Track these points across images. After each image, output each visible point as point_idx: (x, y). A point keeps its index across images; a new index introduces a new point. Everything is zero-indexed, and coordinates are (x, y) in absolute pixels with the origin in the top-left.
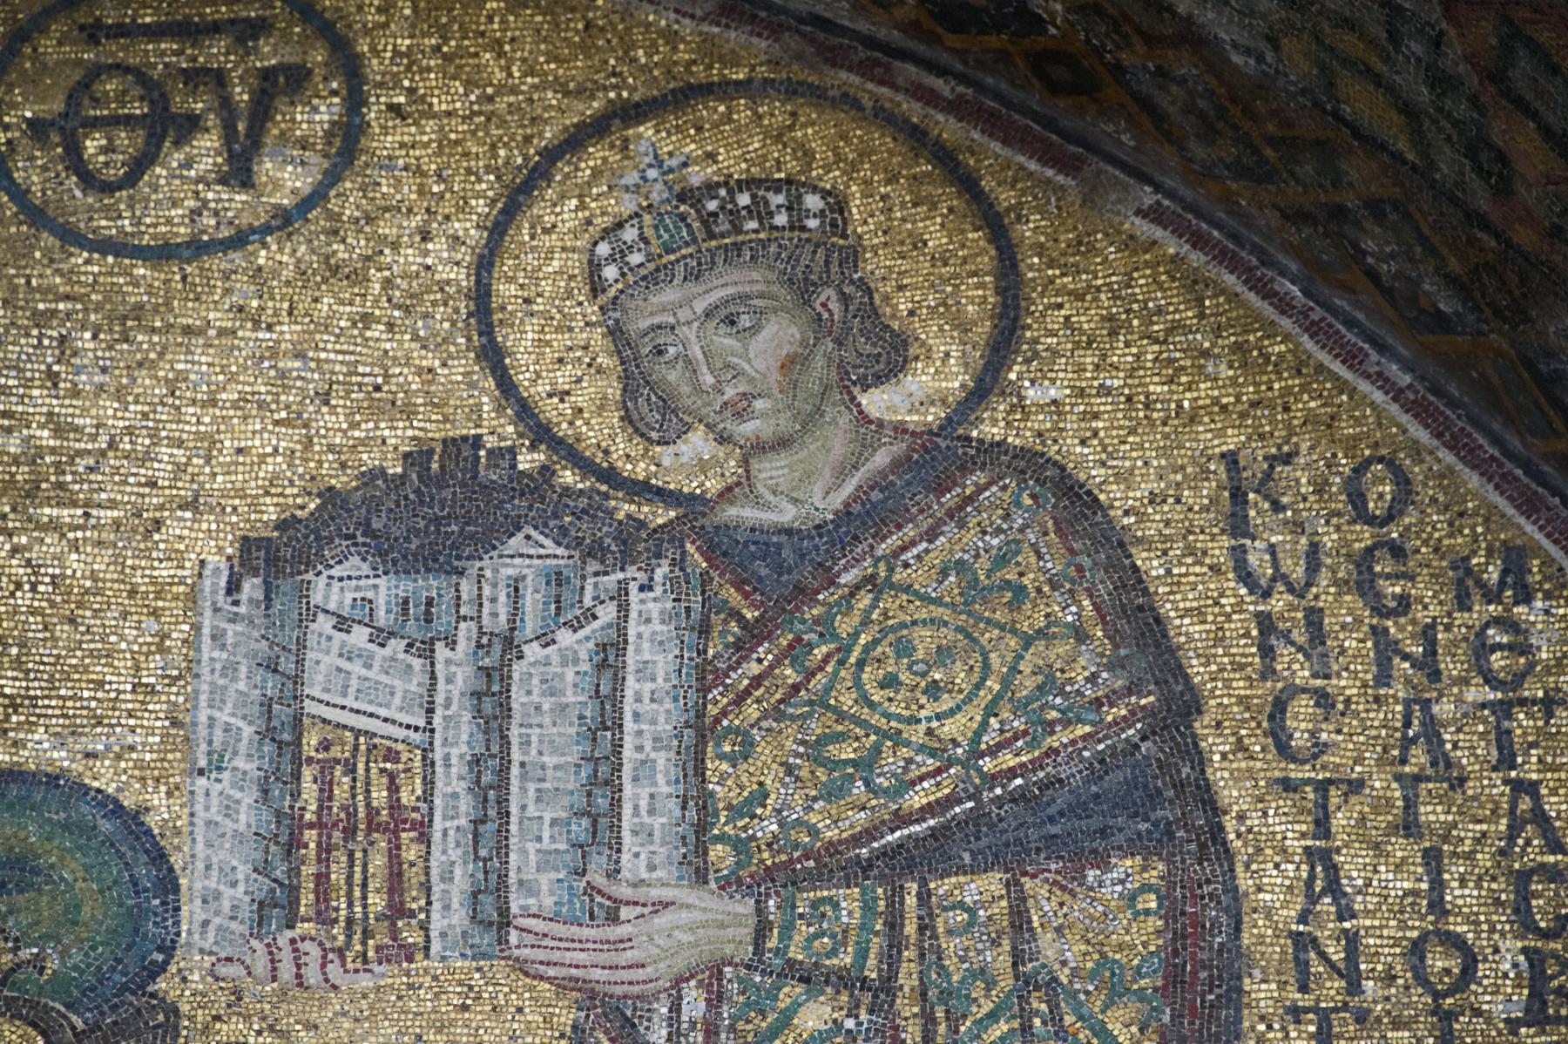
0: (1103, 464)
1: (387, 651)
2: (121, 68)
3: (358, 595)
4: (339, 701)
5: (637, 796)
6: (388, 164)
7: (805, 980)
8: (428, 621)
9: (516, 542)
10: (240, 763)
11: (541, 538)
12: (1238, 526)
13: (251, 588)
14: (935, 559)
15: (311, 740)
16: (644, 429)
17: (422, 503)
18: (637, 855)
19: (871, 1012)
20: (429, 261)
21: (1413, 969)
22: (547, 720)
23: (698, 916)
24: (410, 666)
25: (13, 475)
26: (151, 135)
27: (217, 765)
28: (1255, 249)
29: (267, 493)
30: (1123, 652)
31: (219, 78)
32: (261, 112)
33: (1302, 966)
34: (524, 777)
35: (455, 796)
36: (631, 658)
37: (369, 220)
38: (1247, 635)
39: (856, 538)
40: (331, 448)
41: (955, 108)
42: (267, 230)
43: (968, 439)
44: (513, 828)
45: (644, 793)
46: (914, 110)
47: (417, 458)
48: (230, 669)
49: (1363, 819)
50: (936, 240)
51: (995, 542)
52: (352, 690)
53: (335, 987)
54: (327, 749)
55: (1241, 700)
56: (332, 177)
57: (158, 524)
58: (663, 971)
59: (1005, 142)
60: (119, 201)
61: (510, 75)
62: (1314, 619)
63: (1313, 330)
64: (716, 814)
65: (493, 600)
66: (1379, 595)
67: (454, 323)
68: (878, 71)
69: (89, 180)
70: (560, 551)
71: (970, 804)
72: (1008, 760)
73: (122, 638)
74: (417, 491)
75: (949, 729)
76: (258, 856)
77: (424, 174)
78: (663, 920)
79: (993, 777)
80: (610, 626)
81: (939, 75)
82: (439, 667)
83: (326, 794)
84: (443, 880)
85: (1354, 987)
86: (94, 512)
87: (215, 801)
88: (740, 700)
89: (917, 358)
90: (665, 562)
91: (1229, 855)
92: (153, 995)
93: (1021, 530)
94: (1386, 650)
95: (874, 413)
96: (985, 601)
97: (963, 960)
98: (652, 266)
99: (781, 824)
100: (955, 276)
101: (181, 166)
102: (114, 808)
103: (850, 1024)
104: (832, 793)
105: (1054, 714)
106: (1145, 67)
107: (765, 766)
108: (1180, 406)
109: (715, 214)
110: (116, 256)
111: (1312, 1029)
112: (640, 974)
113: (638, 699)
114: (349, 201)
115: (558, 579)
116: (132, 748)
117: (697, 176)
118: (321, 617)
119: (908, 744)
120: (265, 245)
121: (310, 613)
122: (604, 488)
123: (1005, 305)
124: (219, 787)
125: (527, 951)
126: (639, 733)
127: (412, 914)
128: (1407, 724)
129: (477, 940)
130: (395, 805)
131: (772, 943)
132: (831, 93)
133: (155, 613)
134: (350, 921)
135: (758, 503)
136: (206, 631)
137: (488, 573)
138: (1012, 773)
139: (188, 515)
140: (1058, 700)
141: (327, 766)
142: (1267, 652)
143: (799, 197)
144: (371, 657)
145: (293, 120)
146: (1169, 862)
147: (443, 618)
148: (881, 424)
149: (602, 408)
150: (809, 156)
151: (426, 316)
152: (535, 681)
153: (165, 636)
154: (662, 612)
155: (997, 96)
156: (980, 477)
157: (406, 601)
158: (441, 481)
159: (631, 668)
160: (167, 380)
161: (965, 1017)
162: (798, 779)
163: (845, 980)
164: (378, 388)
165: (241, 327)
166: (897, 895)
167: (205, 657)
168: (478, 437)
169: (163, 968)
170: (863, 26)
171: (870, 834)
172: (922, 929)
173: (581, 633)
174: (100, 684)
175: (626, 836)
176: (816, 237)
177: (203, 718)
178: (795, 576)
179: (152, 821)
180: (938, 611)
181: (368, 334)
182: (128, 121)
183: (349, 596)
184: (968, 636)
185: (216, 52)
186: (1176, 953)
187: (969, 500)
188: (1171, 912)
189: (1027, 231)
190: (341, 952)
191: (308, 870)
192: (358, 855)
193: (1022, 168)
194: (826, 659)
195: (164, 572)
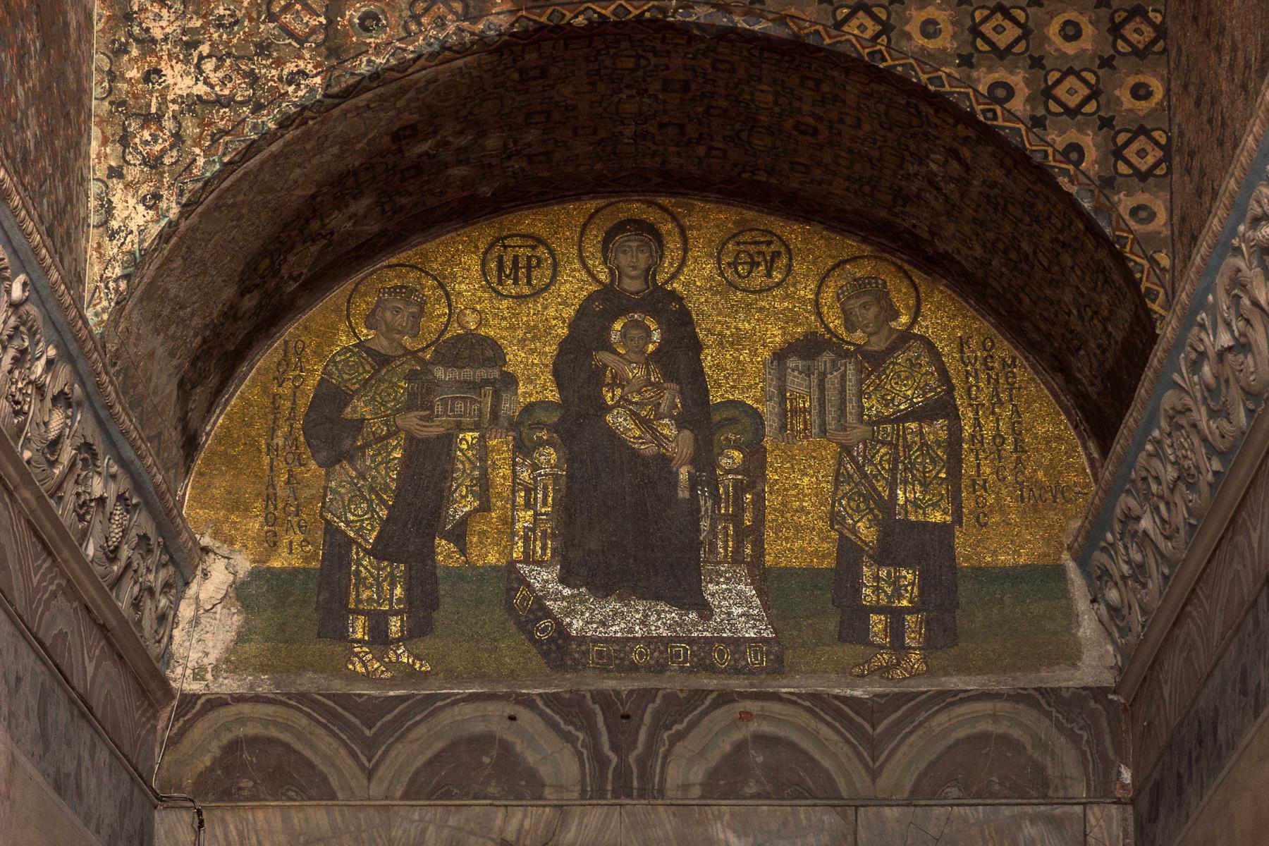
75: (909, 393)
85: (983, 445)
91: (960, 419)
102: (750, 406)
104: (887, 406)
171: (894, 413)
188: (949, 429)
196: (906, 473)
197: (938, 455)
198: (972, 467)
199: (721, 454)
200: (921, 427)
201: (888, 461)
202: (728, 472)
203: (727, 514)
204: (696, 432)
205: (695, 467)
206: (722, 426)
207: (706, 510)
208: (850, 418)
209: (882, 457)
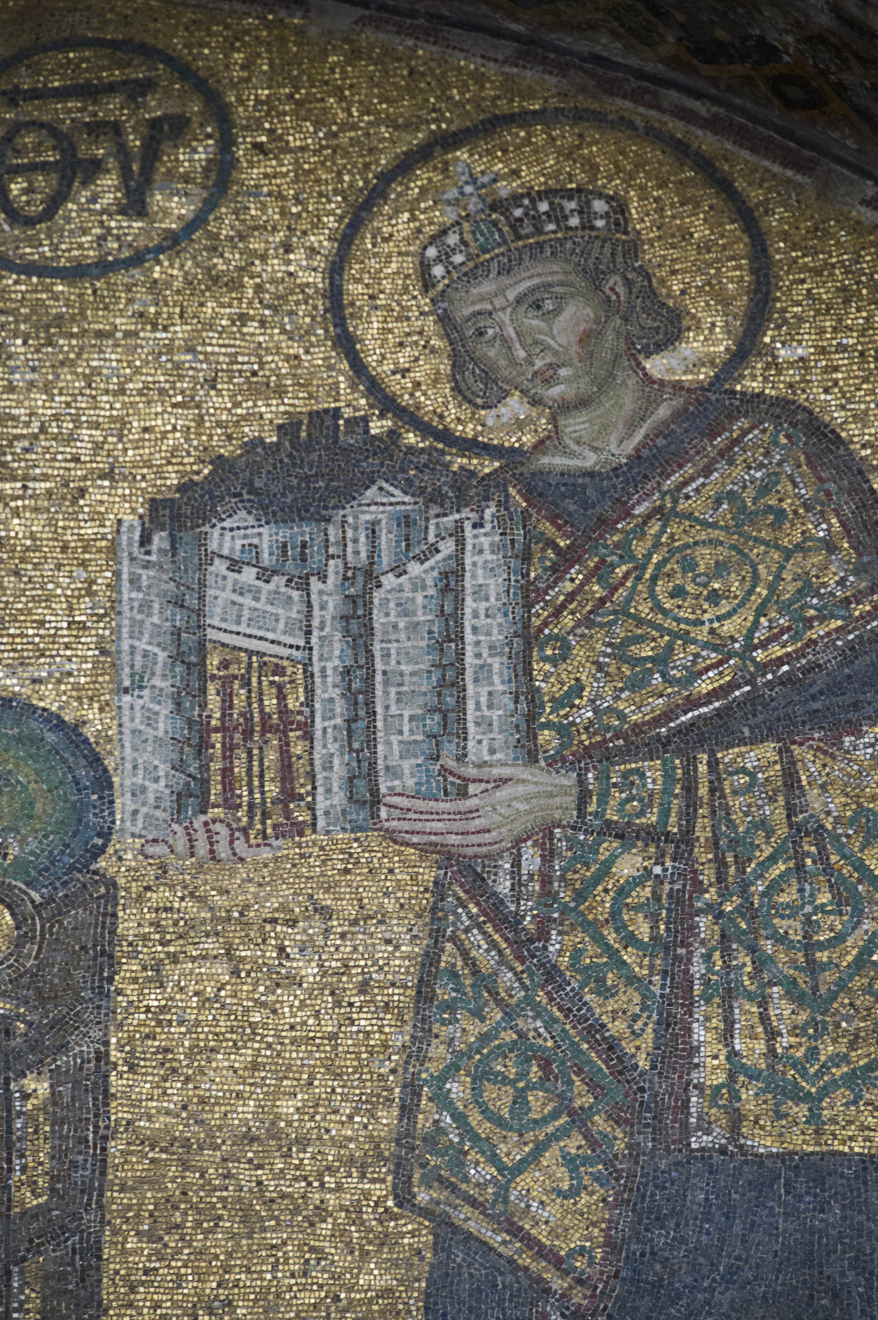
0: (843, 407)
1: (271, 586)
3: (246, 542)
4: (235, 628)
5: (478, 694)
6: (255, 192)
7: (620, 836)
8: (304, 560)
9: (371, 493)
10: (157, 682)
11: (391, 489)
13: (159, 540)
14: (710, 491)
15: (213, 661)
16: (471, 397)
18: (480, 742)
19: (674, 860)
20: (292, 269)
22: (403, 636)
23: (532, 788)
24: (290, 598)
26: (63, 177)
29: (169, 463)
30: (865, 559)
31: (116, 129)
34: (386, 683)
35: (331, 700)
36: (468, 583)
37: (242, 237)
39: (646, 477)
40: (219, 424)
41: (712, 125)
42: (160, 249)
43: (734, 392)
44: (380, 724)
45: (484, 691)
46: (677, 128)
48: (145, 607)
51: (759, 475)
52: (244, 619)
53: (242, 860)
54: (226, 667)
56: (210, 205)
57: (82, 492)
58: (505, 834)
59: (753, 150)
60: (39, 232)
61: (350, 115)
65: (355, 541)
67: (313, 318)
68: (648, 97)
70: (407, 499)
71: (747, 688)
72: (777, 651)
73: (58, 585)
74: (290, 456)
75: (727, 628)
76: (175, 756)
77: (284, 199)
78: (503, 793)
79: (765, 665)
80: (450, 557)
82: (314, 597)
83: (227, 704)
84: (324, 769)
86: (31, 484)
87: (138, 714)
88: (558, 612)
89: (689, 329)
90: (492, 504)
92: (95, 872)
93: (780, 464)
95: (656, 375)
96: (752, 523)
97: (746, 814)
98: (471, 264)
99: (595, 711)
100: (717, 260)
101: (88, 201)
102: (56, 722)
103: (658, 870)
104: (636, 684)
105: (812, 612)
106: (862, 84)
109: (520, 220)
110: (39, 276)
112: (487, 838)
115: (406, 521)
116: (70, 674)
117: (504, 189)
118: (217, 561)
119: (695, 642)
120: (159, 262)
121: (210, 558)
122: (440, 446)
123: (758, 283)
124: (141, 702)
125: (395, 823)
126: (478, 643)
129: (354, 816)
130: (283, 710)
131: (592, 808)
132: (610, 117)
133: (84, 564)
134: (251, 805)
135: (566, 452)
136: (125, 576)
137: (350, 520)
138: (780, 662)
139: (106, 483)
140: (815, 601)
143: (588, 203)
144: (259, 591)
145: (177, 160)
147: (316, 559)
148: (662, 383)
149: (436, 381)
150: (593, 169)
151: (291, 313)
152: (392, 605)
153: (93, 582)
154: (492, 544)
155: (745, 113)
156: (743, 423)
157: (285, 545)
158: (309, 447)
159: (468, 591)
160: (84, 375)
161: (750, 860)
162: (607, 674)
165: (143, 329)
166: (691, 764)
167: (125, 597)
168: (337, 410)
169: (102, 850)
170: (633, 61)
171: (667, 715)
172: (712, 791)
173: (427, 565)
174: (41, 623)
176: (602, 234)
177: (125, 647)
178: (598, 510)
179: (89, 732)
180: (716, 533)
181: (245, 330)
182: (44, 167)
183: (239, 543)
184: (740, 552)
187: (736, 442)
190: (245, 831)
192: (256, 751)
193: (767, 170)
194: (626, 576)
195: (89, 531)
196: (727, 953)
209: (622, 892)
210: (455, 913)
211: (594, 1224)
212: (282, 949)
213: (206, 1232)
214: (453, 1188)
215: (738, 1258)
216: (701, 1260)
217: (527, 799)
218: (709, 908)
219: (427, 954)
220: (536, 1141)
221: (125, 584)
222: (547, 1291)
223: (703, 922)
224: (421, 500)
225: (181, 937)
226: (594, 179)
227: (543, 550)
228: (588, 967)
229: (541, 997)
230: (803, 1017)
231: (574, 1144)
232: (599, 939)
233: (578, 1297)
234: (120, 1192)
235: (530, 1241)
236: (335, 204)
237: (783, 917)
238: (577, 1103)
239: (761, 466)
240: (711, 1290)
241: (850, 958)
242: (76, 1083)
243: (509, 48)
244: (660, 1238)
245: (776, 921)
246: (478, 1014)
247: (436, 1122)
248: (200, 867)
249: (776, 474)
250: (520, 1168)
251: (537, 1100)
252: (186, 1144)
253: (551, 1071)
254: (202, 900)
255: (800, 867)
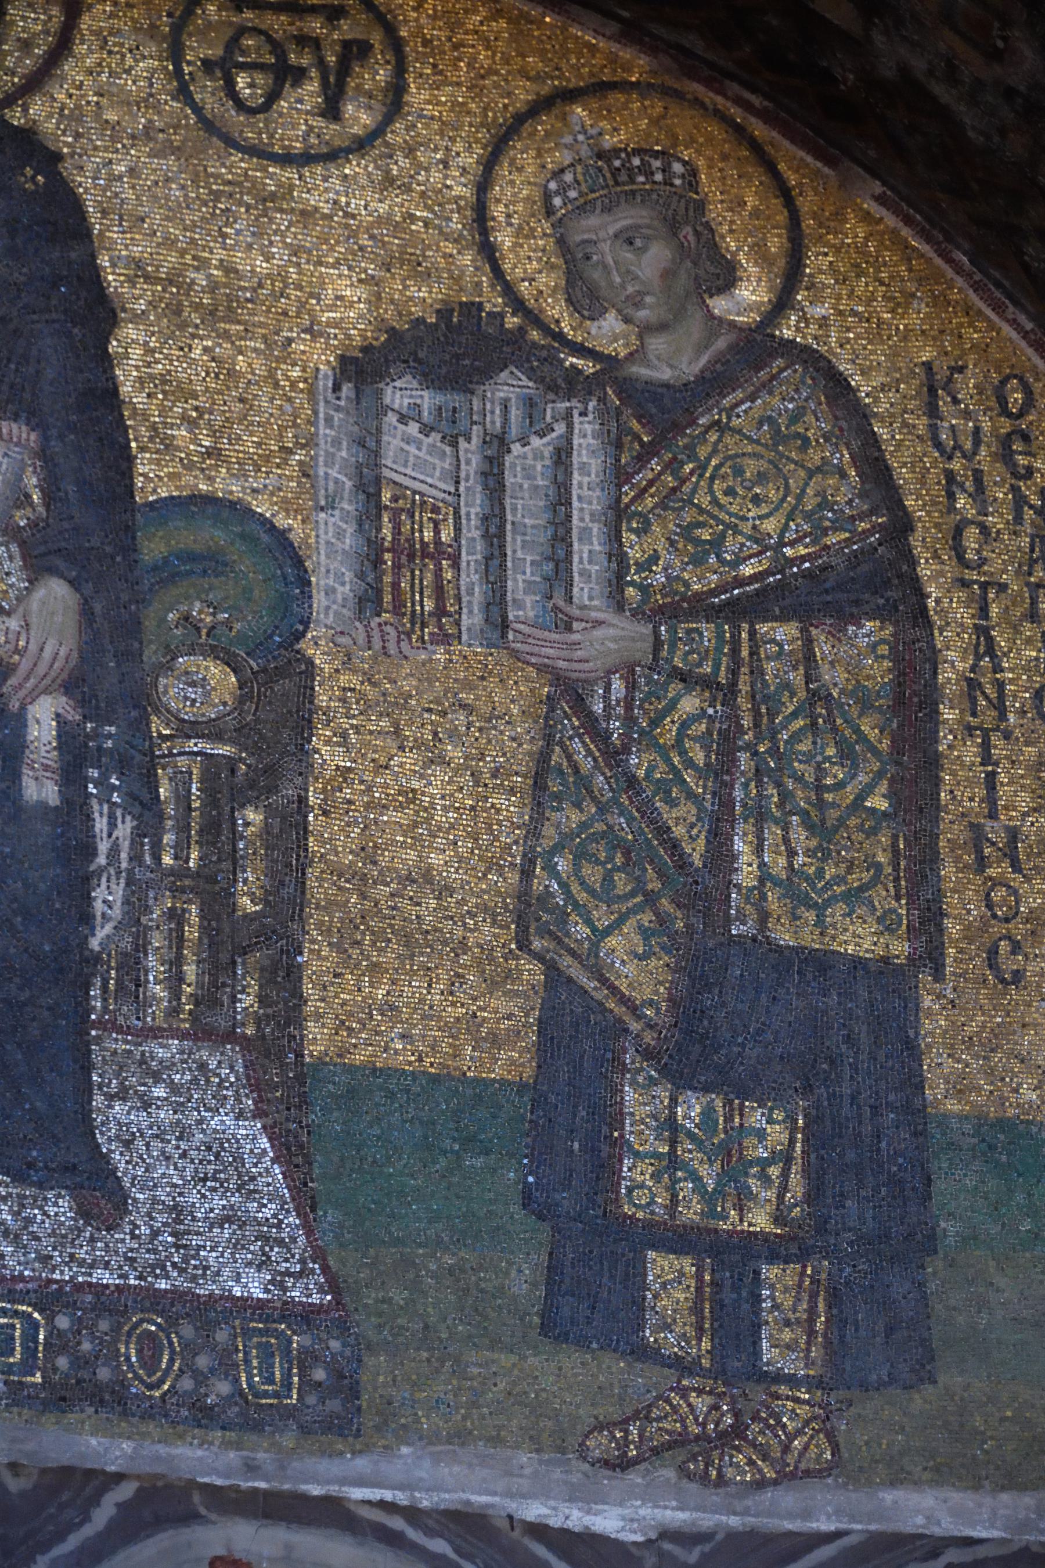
0: (854, 362)
1: (430, 440)
2: (257, 31)
3: (412, 401)
5: (581, 551)
7: (683, 680)
8: (454, 422)
12: (933, 411)
13: (347, 389)
14: (756, 413)
15: (386, 496)
17: (448, 343)
18: (582, 589)
20: (448, 182)
21: (1036, 707)
22: (527, 495)
24: (444, 453)
25: (201, 299)
27: (330, 506)
28: (942, 230)
30: (867, 487)
31: (315, 44)
32: (344, 70)
33: (973, 701)
34: (514, 531)
35: (474, 539)
38: (939, 483)
39: (708, 394)
40: (392, 301)
41: (763, 115)
42: (349, 151)
43: (773, 336)
44: (509, 564)
45: (586, 549)
47: (444, 313)
48: (336, 443)
49: (1007, 608)
50: (751, 201)
51: (791, 406)
52: (410, 464)
53: (406, 657)
54: (396, 501)
55: (937, 526)
57: (290, 341)
59: (793, 141)
60: (259, 121)
61: (494, 62)
62: (978, 476)
63: (976, 287)
64: (629, 567)
65: (492, 412)
66: (1015, 465)
67: (464, 226)
69: (240, 105)
70: (531, 384)
71: (779, 577)
74: (445, 336)
76: (358, 567)
78: (599, 633)
80: (561, 436)
81: (753, 92)
82: (461, 453)
84: (468, 594)
85: (1003, 716)
87: (331, 529)
89: (741, 279)
91: (929, 624)
92: (298, 652)
93: (806, 400)
94: (1020, 502)
97: (776, 676)
98: (582, 200)
99: (667, 577)
102: (269, 526)
103: (711, 711)
104: (698, 561)
105: (828, 524)
107: (657, 539)
108: (898, 329)
109: (618, 169)
110: (259, 158)
111: (979, 740)
113: (580, 486)
114: (397, 134)
115: (530, 403)
117: (609, 141)
118: (390, 413)
119: (741, 533)
120: (349, 161)
121: (386, 409)
122: (556, 345)
123: (793, 249)
124: (333, 519)
126: (582, 510)
127: (451, 616)
128: (1032, 551)
130: (437, 541)
131: (664, 654)
132: (689, 96)
133: (290, 400)
136: (321, 415)
137: (489, 395)
138: (803, 559)
139: (308, 337)
140: (830, 515)
141: (396, 513)
142: (951, 496)
143: (669, 164)
146: (896, 624)
147: (463, 424)
148: (720, 320)
150: (675, 137)
152: (519, 469)
154: (593, 431)
156: (779, 362)
157: (440, 408)
159: (575, 466)
161: (778, 714)
162: (677, 550)
163: (708, 683)
164: (419, 264)
167: (321, 432)
168: (481, 304)
169: (303, 634)
172: (751, 654)
173: (545, 440)
175: (576, 575)
176: (679, 191)
177: (321, 473)
181: (413, 227)
183: (406, 401)
184: (776, 467)
185: (316, 26)
186: (899, 684)
187: (773, 377)
188: (895, 656)
189: (806, 203)
191: (388, 579)
192: (417, 572)
193: (802, 159)
194: (692, 473)
195: (296, 373)
197: (862, 738)
198: (971, 783)
199: (168, 667)
200: (809, 642)
201: (704, 740)
202: (188, 729)
203: (179, 872)
204: (88, 588)
205: (82, 702)
206: (174, 577)
207: (114, 852)
208: (582, 591)
209: (684, 725)
210: (562, 723)
211: (661, 983)
212: (435, 734)
213: (380, 950)
214: (560, 942)
215: (763, 1024)
216: (737, 1022)
217: (615, 640)
218: (748, 747)
219: (541, 753)
220: (620, 912)
221: (322, 422)
222: (626, 1030)
223: (743, 757)
224: (541, 387)
225: (361, 714)
226: (675, 145)
227: (631, 442)
228: (658, 780)
229: (624, 799)
230: (813, 843)
231: (647, 918)
232: (668, 761)
233: (649, 1038)
234: (316, 909)
235: (614, 989)
236: (482, 135)
237: (800, 762)
238: (650, 887)
239: (792, 400)
240: (743, 1045)
241: (848, 801)
242: (284, 819)
243: (614, 27)
244: (708, 1000)
245: (796, 764)
246: (578, 805)
247: (547, 887)
248: (374, 658)
249: (804, 408)
250: (608, 932)
251: (620, 878)
252: (364, 878)
253: (630, 859)
254: (374, 684)
255: (814, 724)
